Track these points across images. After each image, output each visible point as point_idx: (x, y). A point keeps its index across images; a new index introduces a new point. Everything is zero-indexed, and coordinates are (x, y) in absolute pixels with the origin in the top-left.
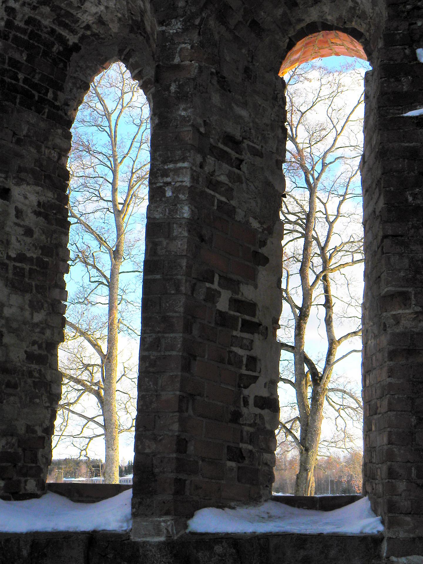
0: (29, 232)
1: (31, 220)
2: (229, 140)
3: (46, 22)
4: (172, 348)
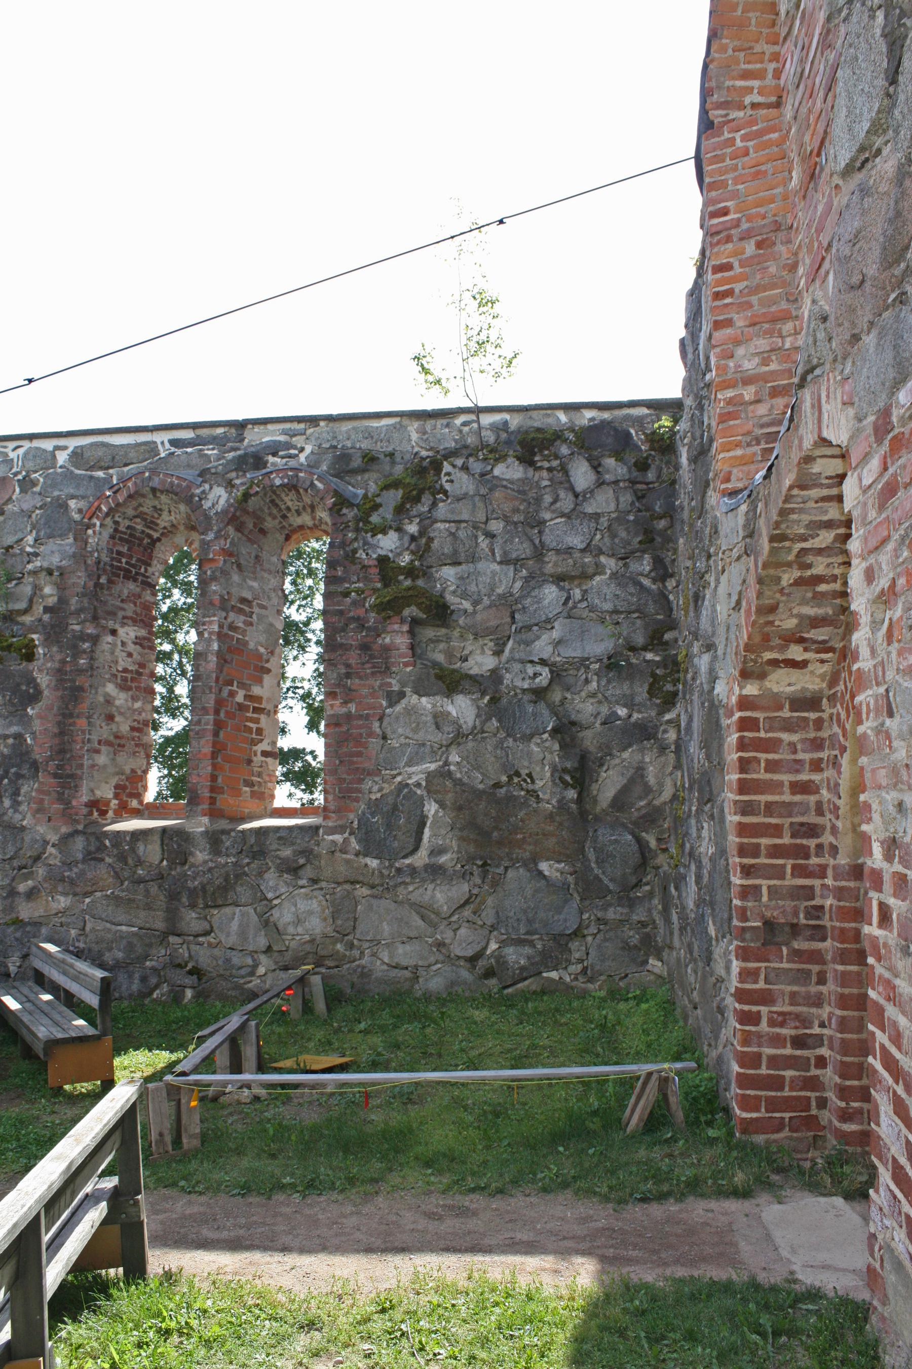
0: (130, 655)
1: (131, 647)
2: (243, 600)
3: (139, 527)
4: (207, 724)
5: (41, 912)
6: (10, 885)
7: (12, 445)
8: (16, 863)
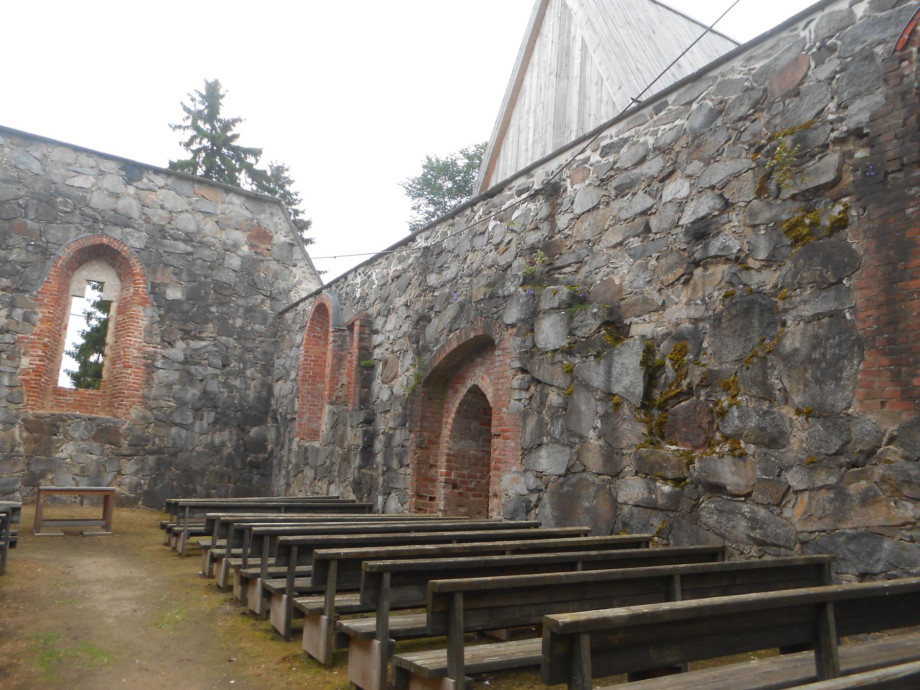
5: (881, 520)
6: (837, 484)
7: (802, 24)
8: (843, 460)
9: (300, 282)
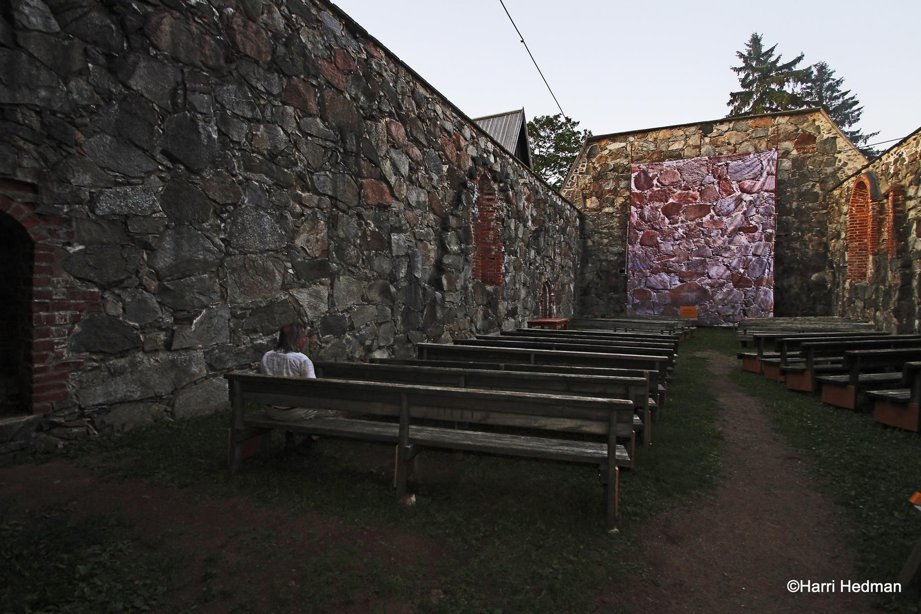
9: (845, 164)
